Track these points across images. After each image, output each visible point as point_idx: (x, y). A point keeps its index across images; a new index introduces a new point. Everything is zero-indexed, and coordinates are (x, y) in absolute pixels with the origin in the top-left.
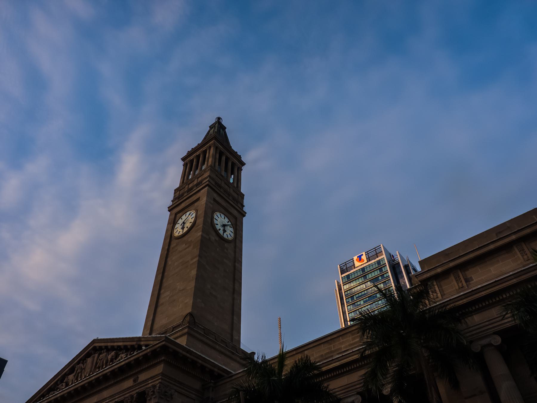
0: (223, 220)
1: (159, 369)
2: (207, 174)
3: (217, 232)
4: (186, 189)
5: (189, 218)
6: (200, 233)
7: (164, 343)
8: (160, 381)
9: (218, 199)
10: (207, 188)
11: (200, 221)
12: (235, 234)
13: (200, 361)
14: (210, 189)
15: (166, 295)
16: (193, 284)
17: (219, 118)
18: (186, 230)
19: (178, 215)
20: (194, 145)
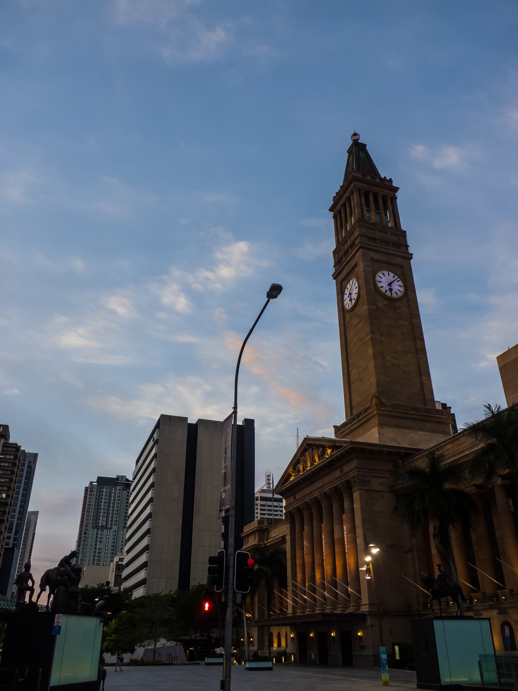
0: (388, 277)
1: (354, 464)
2: (357, 233)
3: (383, 295)
4: (343, 252)
5: (353, 288)
6: (366, 307)
7: (350, 446)
8: (356, 473)
9: (376, 256)
10: (360, 250)
11: (363, 292)
12: (406, 286)
13: (386, 449)
14: (364, 250)
15: (354, 373)
16: (372, 364)
17: (355, 134)
18: (354, 302)
19: (344, 283)
20: (338, 189)
